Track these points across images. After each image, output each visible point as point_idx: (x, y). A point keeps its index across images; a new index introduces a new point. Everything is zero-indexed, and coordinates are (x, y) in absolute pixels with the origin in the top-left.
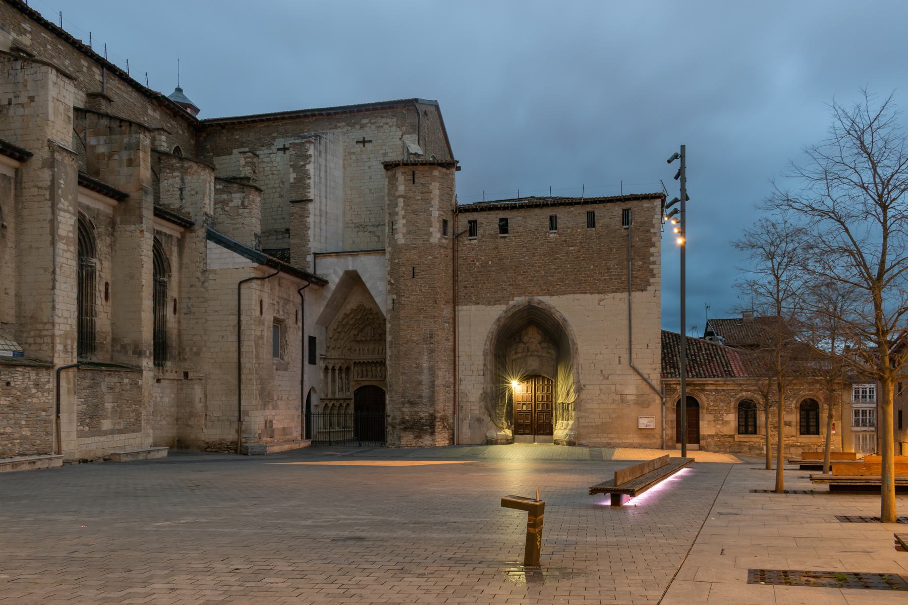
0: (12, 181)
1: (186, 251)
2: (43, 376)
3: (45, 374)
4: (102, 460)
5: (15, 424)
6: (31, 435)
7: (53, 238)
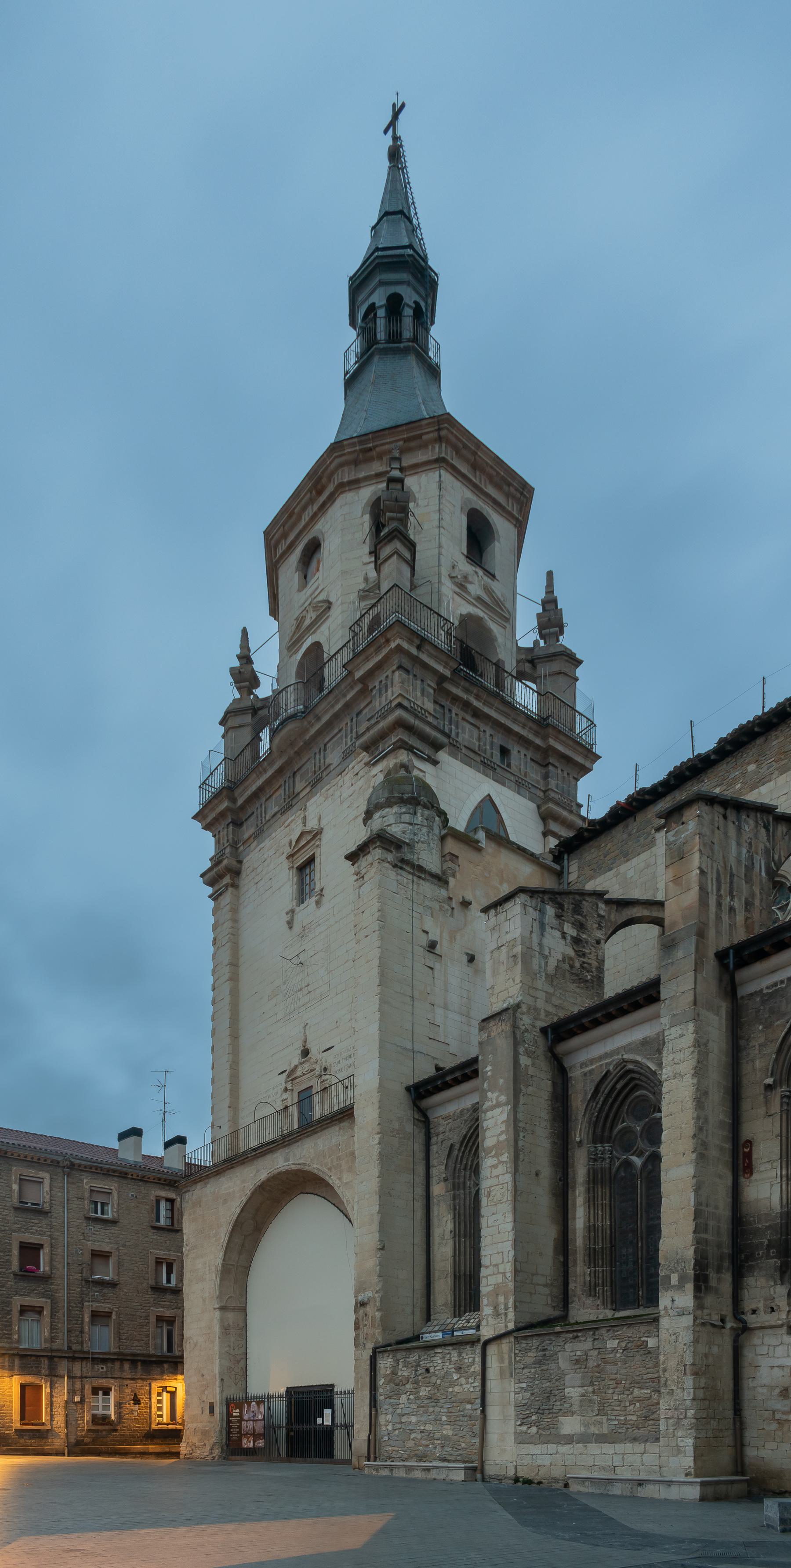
2: (467, 1355)
3: (470, 1352)
5: (435, 1420)
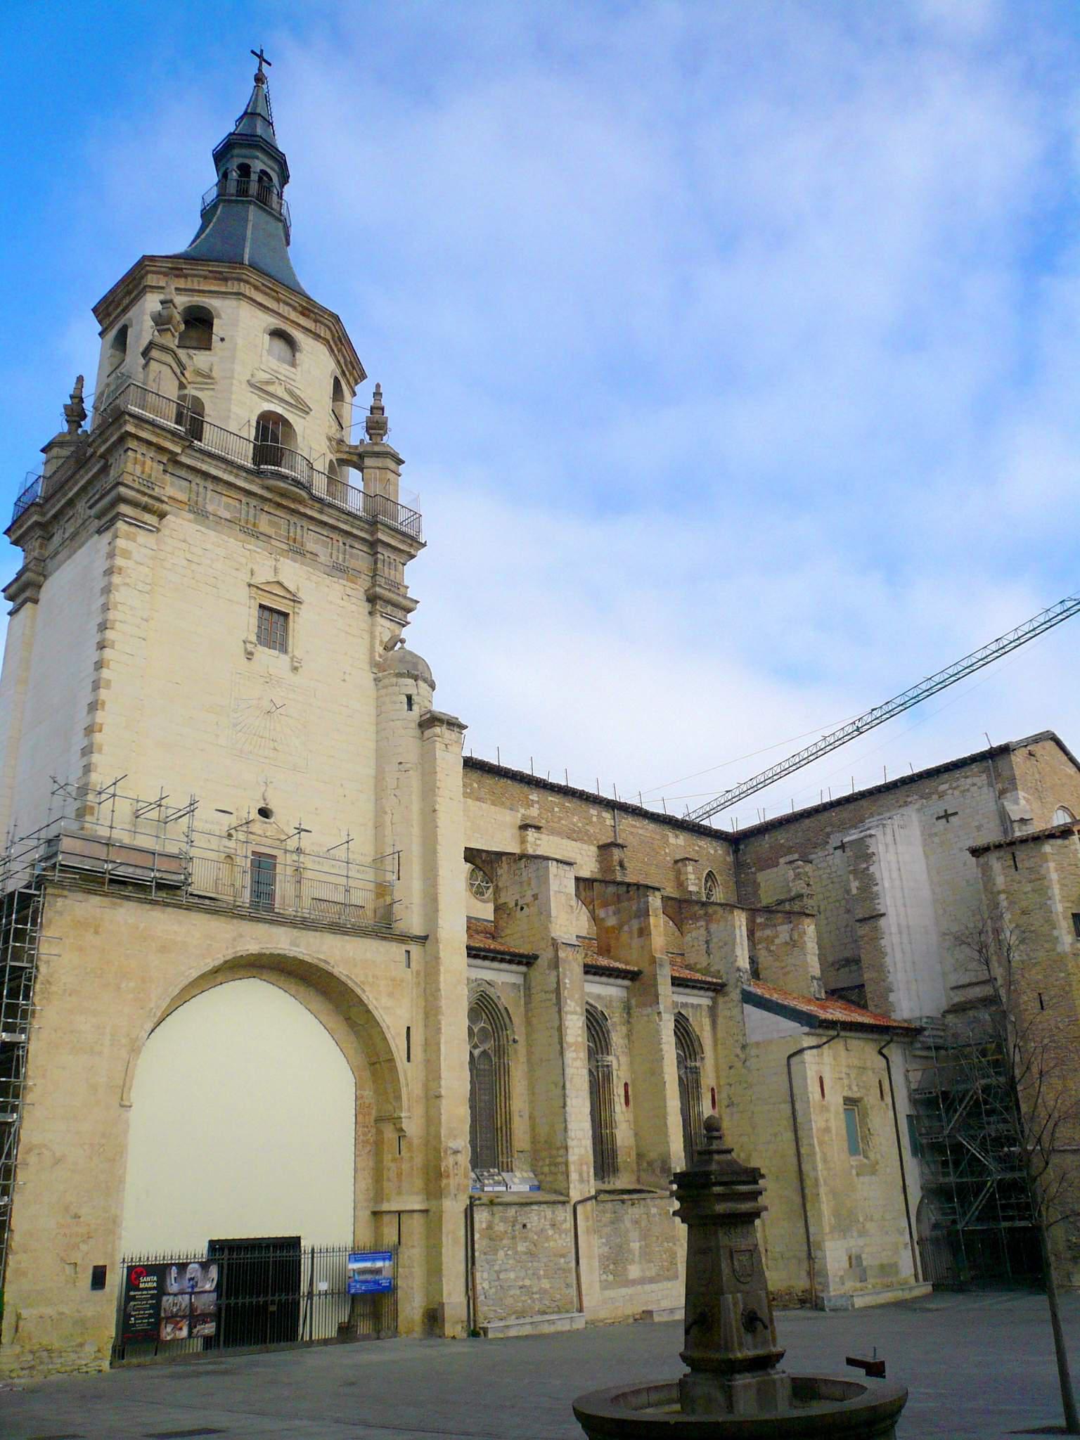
0: (522, 988)
1: (720, 1021)
4: (631, 1320)
5: (534, 1274)
6: (551, 1288)
7: (562, 1047)
